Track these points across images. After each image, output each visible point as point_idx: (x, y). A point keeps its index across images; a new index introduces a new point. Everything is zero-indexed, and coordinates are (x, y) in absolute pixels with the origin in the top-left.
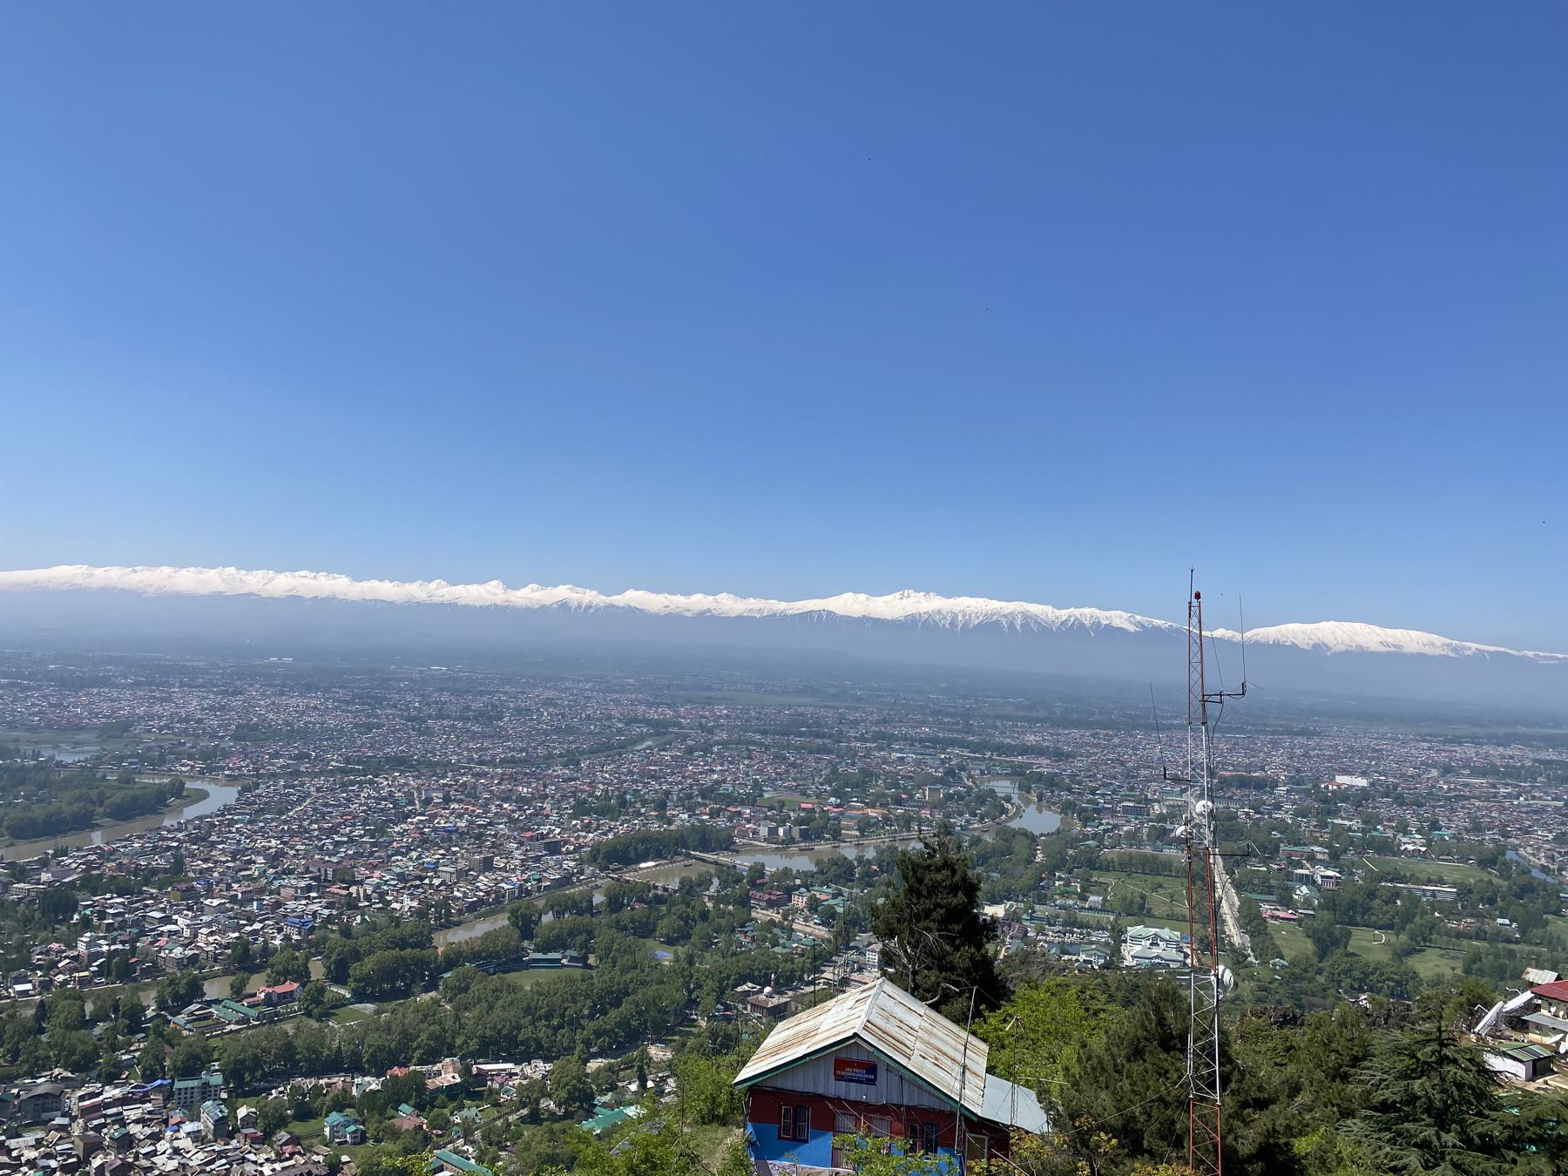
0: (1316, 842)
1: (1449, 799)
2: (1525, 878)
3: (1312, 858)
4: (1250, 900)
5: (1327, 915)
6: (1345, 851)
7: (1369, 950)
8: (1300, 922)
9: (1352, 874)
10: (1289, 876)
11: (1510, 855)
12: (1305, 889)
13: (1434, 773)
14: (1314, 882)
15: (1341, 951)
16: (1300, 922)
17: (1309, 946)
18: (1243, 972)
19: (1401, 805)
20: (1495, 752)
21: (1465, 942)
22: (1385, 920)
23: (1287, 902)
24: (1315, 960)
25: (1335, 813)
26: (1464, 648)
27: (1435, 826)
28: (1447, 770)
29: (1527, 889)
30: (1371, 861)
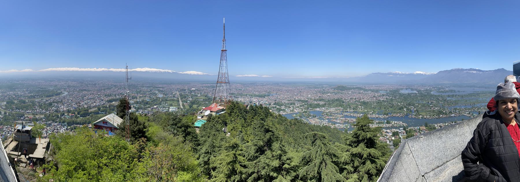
30: (195, 97)
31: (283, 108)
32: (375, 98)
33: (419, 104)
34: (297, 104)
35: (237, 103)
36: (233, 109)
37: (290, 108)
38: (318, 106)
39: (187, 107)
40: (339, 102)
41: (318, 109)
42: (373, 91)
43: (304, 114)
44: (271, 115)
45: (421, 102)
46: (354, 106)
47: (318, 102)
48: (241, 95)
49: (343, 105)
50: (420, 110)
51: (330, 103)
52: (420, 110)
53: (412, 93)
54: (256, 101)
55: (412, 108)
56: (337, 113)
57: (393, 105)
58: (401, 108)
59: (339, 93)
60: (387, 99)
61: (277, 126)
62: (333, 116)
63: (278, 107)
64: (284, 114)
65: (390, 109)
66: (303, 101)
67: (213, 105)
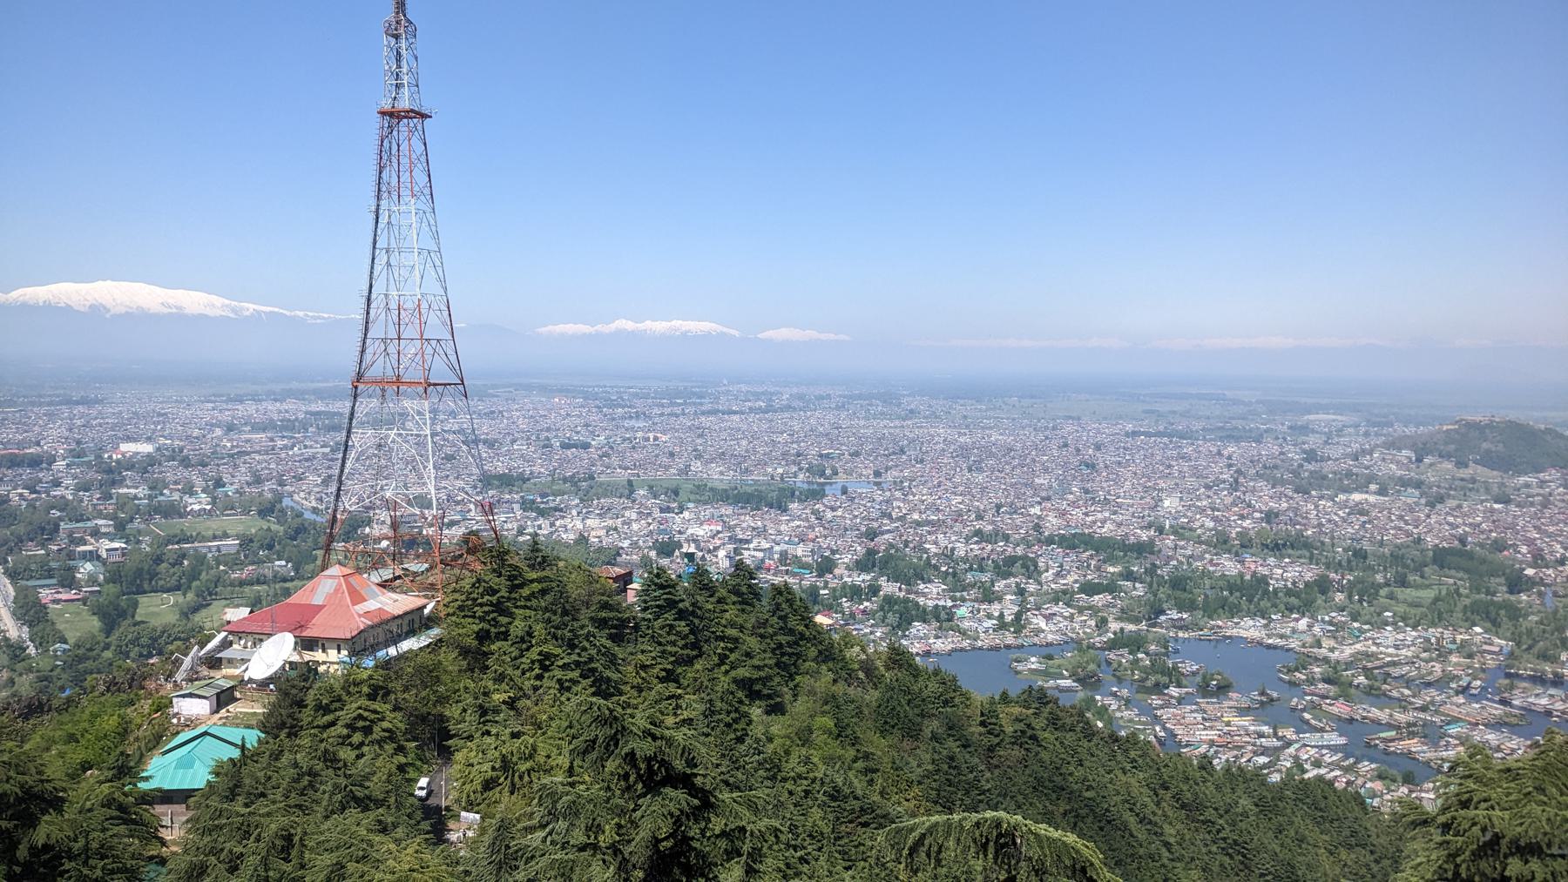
0: (100, 515)
1: (232, 456)
2: (296, 523)
3: (96, 533)
4: (27, 588)
5: (112, 589)
6: (132, 520)
7: (154, 614)
8: (84, 601)
9: (139, 542)
10: (71, 556)
11: (286, 502)
12: (89, 566)
13: (218, 432)
14: (99, 557)
15: (129, 621)
16: (84, 601)
17: (95, 623)
18: (19, 666)
19: (186, 467)
20: (271, 407)
21: (247, 589)
22: (173, 582)
23: (69, 581)
24: (101, 637)
25: (120, 482)
26: (242, 309)
27: (219, 483)
28: (230, 428)
29: (300, 531)
31: (932, 594)
34: (1060, 570)
35: (539, 556)
36: (499, 608)
37: (989, 596)
38: (1251, 595)
39: (76, 623)
41: (1249, 628)
44: (829, 654)
47: (1255, 565)
48: (587, 489)
49: (1515, 613)
51: (1371, 579)
54: (708, 539)
56: (1441, 683)
59: (1468, 487)
61: (878, 745)
62: (1403, 704)
64: (940, 645)
66: (1107, 548)
67: (324, 587)
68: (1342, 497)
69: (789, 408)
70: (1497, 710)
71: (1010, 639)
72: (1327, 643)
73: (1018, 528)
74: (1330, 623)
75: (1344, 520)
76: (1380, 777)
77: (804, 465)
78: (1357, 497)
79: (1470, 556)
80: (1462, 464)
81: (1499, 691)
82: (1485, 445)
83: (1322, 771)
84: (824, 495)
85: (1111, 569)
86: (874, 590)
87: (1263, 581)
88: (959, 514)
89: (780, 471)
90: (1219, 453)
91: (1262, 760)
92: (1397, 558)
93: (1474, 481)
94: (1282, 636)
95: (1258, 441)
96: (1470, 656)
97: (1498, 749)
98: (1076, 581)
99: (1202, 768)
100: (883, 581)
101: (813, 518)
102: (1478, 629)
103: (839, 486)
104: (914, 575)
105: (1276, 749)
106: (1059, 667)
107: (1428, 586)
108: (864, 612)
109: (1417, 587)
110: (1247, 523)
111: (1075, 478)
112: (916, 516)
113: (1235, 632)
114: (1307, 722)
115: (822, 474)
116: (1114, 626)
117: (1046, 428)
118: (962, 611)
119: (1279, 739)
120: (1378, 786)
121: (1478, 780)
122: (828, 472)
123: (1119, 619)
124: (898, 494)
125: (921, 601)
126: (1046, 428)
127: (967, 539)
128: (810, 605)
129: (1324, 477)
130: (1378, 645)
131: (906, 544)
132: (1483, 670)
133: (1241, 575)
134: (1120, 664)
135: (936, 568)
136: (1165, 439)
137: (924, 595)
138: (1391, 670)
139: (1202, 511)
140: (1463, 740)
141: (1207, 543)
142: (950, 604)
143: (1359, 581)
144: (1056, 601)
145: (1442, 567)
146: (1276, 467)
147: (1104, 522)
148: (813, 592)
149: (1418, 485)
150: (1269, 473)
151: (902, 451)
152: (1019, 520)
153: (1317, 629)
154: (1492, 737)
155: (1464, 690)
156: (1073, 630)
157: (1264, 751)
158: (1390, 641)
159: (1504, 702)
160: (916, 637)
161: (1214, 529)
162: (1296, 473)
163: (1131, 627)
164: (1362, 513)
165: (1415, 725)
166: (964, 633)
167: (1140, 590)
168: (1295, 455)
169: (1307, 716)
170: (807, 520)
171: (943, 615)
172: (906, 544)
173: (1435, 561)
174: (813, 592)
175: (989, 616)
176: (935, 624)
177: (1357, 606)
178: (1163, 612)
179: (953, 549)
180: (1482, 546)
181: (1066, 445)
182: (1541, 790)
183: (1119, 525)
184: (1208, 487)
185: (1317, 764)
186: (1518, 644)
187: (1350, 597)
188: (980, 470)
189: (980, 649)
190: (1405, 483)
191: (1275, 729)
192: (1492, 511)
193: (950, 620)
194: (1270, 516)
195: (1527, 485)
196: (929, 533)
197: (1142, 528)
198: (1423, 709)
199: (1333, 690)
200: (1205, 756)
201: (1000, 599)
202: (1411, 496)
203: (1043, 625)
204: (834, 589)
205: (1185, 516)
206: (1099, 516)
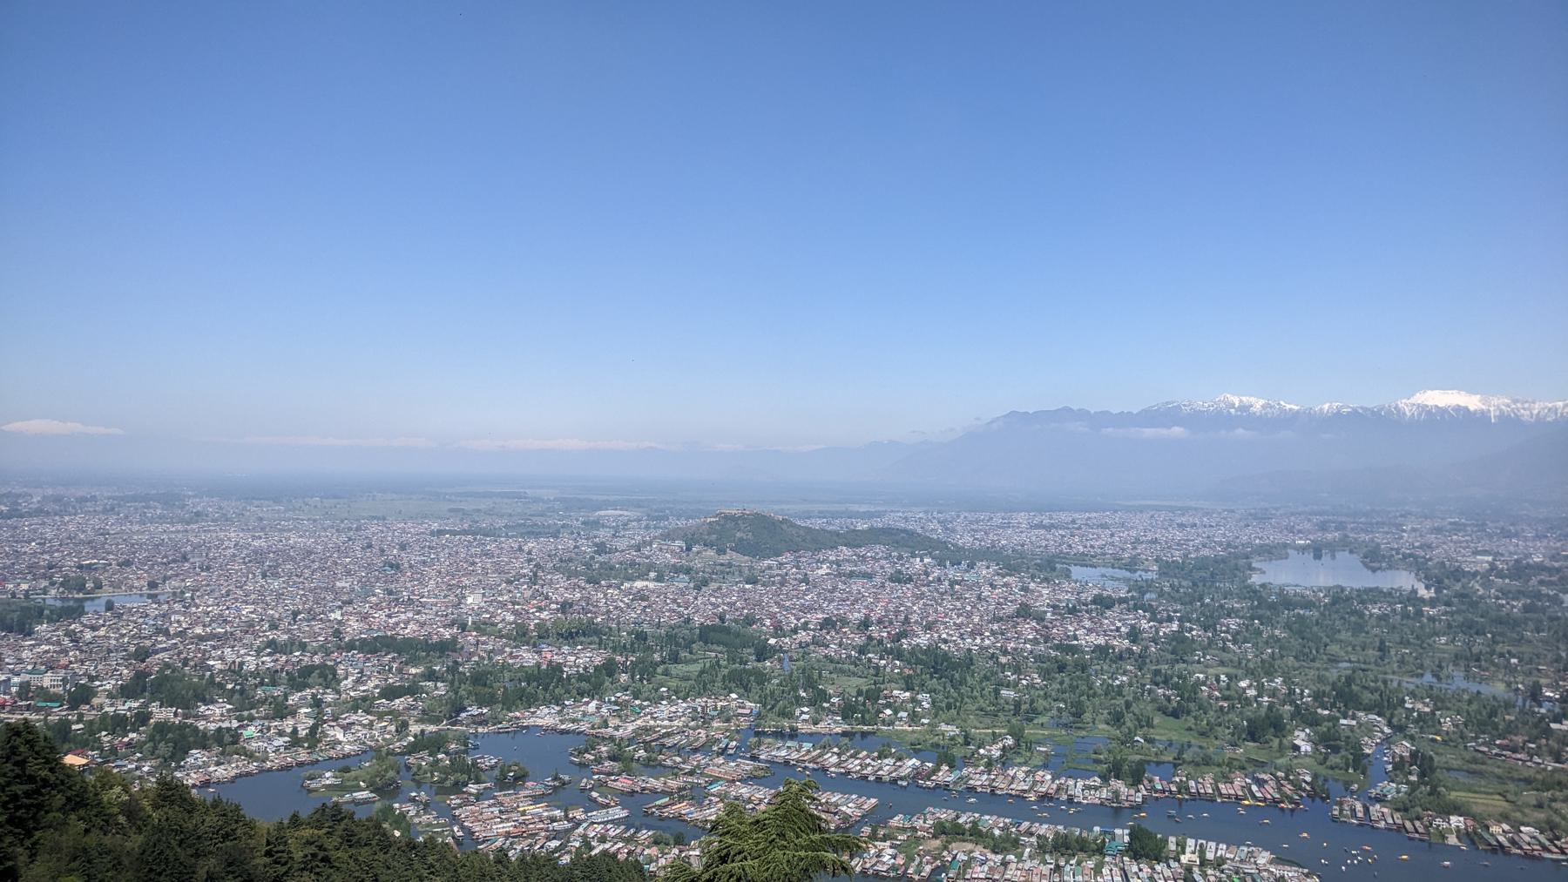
31: (215, 716)
32: (1028, 629)
33: (1440, 702)
34: (358, 677)
37: (282, 711)
38: (548, 684)
40: (730, 654)
41: (545, 717)
42: (1011, 563)
43: (423, 760)
44: (80, 797)
45: (1457, 681)
46: (853, 684)
47: (550, 654)
49: (762, 678)
50: (1450, 758)
51: (647, 659)
52: (1450, 758)
53: (1375, 595)
55: (1370, 731)
56: (704, 749)
57: (1189, 693)
58: (1266, 728)
59: (725, 571)
60: (1134, 635)
62: (675, 771)
63: (161, 713)
64: (221, 772)
65: (1166, 731)
66: (409, 649)
68: (627, 585)
69: (39, 512)
70: (748, 766)
71: (303, 756)
72: (613, 722)
73: (315, 635)
74: (616, 703)
75: (628, 606)
76: (656, 843)
77: (58, 578)
78: (639, 584)
79: (727, 630)
80: (721, 552)
81: (750, 749)
82: (738, 535)
83: (607, 846)
84: (82, 613)
85: (413, 671)
86: (143, 718)
87: (556, 669)
88: (251, 624)
89: (24, 586)
90: (520, 549)
91: (554, 844)
92: (671, 638)
93: (730, 565)
94: (574, 721)
95: (555, 536)
96: (728, 720)
97: (749, 801)
98: (376, 687)
99: (498, 861)
100: (154, 707)
101: (66, 641)
102: (734, 696)
103: (103, 601)
104: (189, 695)
105: (568, 831)
106: (356, 778)
107: (695, 661)
108: (129, 745)
109: (687, 662)
110: (545, 615)
111: (378, 579)
112: (199, 630)
113: (531, 722)
114: (594, 800)
115: (81, 588)
116: (415, 728)
117: (350, 529)
118: (251, 731)
119: (570, 820)
120: (654, 851)
121: (735, 835)
122: (89, 585)
123: (420, 721)
124: (177, 607)
125: (201, 725)
126: (350, 529)
127: (259, 651)
128: (58, 745)
129: (612, 568)
130: (655, 719)
131: (185, 664)
132: (738, 732)
133: (538, 665)
134: (420, 767)
135: (221, 686)
136: (470, 537)
137: (205, 718)
138: (666, 741)
139: (503, 605)
140: (722, 797)
141: (508, 637)
142: (235, 724)
143: (641, 661)
144: (355, 709)
145: (706, 643)
146: (570, 560)
147: (407, 622)
148: (63, 728)
149: (688, 571)
150: (565, 566)
151: (185, 558)
152: (317, 626)
153: (604, 710)
154: (744, 791)
155: (723, 752)
156: (372, 737)
157: (556, 835)
158: (665, 715)
159: (754, 758)
160: (192, 767)
161: (514, 622)
162: (588, 566)
163: (432, 728)
164: (644, 598)
165: (684, 789)
166: (250, 756)
167: (442, 689)
168: (587, 549)
169: (594, 794)
170: (59, 643)
171: (227, 739)
172: (185, 662)
173: (701, 637)
174: (64, 726)
175: (281, 734)
176: (217, 749)
177: (638, 685)
178: (464, 709)
179: (242, 664)
180: (736, 621)
181: (370, 546)
182: (782, 835)
183: (422, 625)
184: (509, 582)
185: (603, 840)
186: (764, 706)
187: (633, 677)
188: (276, 575)
189: (270, 770)
190: (677, 570)
191: (566, 811)
192: (744, 591)
193: (235, 742)
194: (565, 607)
195: (770, 568)
196: (214, 648)
197: (444, 627)
198: (691, 773)
199: (616, 765)
200: (501, 850)
201: (293, 713)
202: (682, 581)
203: (340, 736)
204: (91, 722)
205: (487, 612)
206: (403, 617)
